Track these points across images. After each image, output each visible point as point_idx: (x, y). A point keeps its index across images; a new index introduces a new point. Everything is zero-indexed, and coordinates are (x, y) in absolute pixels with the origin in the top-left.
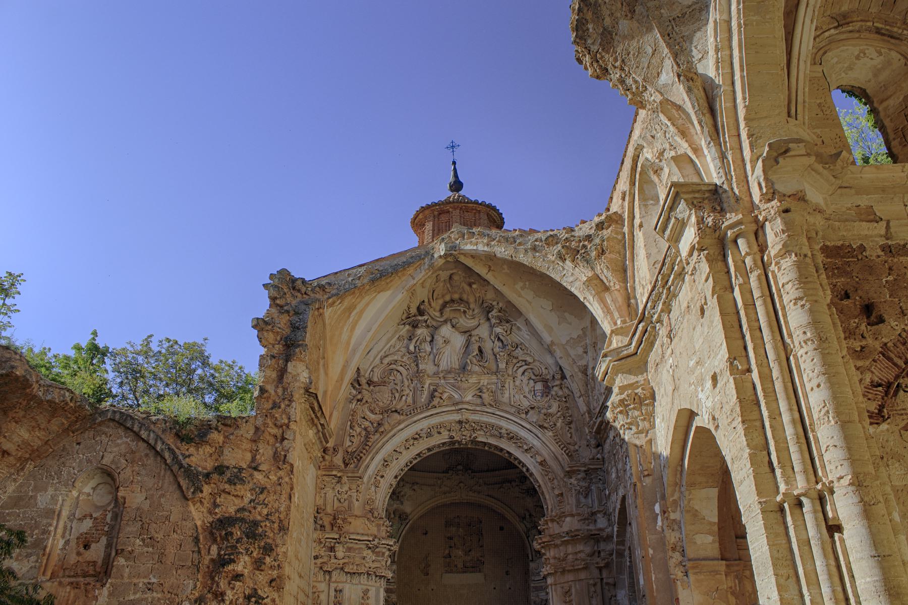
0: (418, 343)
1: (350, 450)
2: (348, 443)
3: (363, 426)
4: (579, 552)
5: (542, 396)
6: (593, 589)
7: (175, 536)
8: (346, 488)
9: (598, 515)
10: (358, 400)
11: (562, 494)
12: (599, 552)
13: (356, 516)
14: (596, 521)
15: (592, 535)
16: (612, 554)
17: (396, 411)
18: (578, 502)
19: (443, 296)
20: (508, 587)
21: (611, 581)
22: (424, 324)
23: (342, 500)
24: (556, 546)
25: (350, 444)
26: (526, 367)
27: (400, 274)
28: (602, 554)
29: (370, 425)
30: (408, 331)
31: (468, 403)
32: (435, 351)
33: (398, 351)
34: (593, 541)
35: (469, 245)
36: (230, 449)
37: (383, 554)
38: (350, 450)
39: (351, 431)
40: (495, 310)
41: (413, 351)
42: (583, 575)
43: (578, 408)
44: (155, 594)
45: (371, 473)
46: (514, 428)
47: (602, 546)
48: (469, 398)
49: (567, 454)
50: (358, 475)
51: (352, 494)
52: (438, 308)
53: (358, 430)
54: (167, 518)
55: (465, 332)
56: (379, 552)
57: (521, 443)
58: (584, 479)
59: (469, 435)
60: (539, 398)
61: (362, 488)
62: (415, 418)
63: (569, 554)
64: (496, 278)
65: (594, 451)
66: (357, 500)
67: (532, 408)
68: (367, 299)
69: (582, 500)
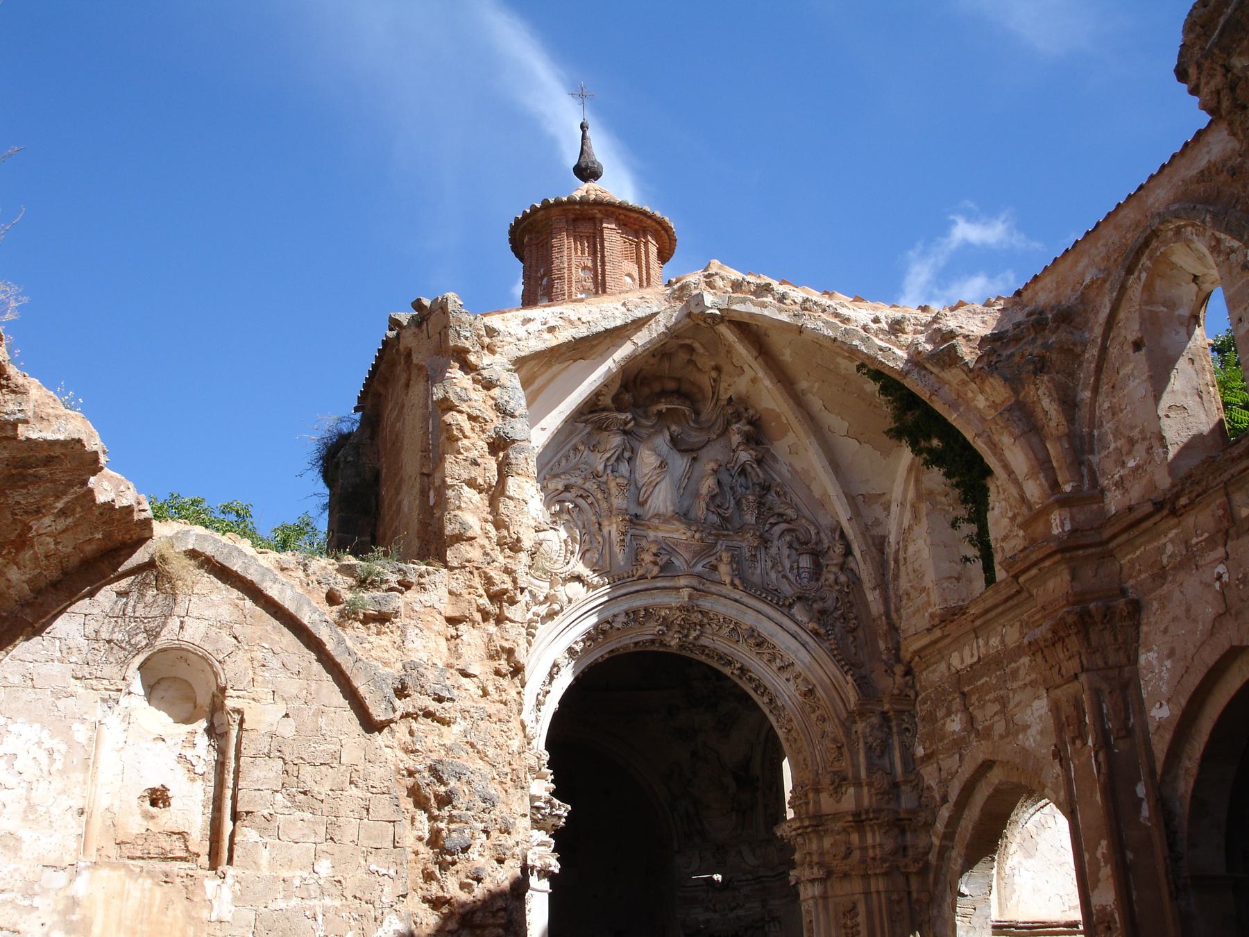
5: (810, 579)
7: (353, 791)
12: (905, 849)
14: (898, 797)
16: (927, 854)
26: (784, 526)
33: (576, 468)
36: (417, 631)
40: (744, 421)
43: (866, 604)
44: (327, 901)
46: (766, 628)
54: (336, 756)
68: (556, 368)
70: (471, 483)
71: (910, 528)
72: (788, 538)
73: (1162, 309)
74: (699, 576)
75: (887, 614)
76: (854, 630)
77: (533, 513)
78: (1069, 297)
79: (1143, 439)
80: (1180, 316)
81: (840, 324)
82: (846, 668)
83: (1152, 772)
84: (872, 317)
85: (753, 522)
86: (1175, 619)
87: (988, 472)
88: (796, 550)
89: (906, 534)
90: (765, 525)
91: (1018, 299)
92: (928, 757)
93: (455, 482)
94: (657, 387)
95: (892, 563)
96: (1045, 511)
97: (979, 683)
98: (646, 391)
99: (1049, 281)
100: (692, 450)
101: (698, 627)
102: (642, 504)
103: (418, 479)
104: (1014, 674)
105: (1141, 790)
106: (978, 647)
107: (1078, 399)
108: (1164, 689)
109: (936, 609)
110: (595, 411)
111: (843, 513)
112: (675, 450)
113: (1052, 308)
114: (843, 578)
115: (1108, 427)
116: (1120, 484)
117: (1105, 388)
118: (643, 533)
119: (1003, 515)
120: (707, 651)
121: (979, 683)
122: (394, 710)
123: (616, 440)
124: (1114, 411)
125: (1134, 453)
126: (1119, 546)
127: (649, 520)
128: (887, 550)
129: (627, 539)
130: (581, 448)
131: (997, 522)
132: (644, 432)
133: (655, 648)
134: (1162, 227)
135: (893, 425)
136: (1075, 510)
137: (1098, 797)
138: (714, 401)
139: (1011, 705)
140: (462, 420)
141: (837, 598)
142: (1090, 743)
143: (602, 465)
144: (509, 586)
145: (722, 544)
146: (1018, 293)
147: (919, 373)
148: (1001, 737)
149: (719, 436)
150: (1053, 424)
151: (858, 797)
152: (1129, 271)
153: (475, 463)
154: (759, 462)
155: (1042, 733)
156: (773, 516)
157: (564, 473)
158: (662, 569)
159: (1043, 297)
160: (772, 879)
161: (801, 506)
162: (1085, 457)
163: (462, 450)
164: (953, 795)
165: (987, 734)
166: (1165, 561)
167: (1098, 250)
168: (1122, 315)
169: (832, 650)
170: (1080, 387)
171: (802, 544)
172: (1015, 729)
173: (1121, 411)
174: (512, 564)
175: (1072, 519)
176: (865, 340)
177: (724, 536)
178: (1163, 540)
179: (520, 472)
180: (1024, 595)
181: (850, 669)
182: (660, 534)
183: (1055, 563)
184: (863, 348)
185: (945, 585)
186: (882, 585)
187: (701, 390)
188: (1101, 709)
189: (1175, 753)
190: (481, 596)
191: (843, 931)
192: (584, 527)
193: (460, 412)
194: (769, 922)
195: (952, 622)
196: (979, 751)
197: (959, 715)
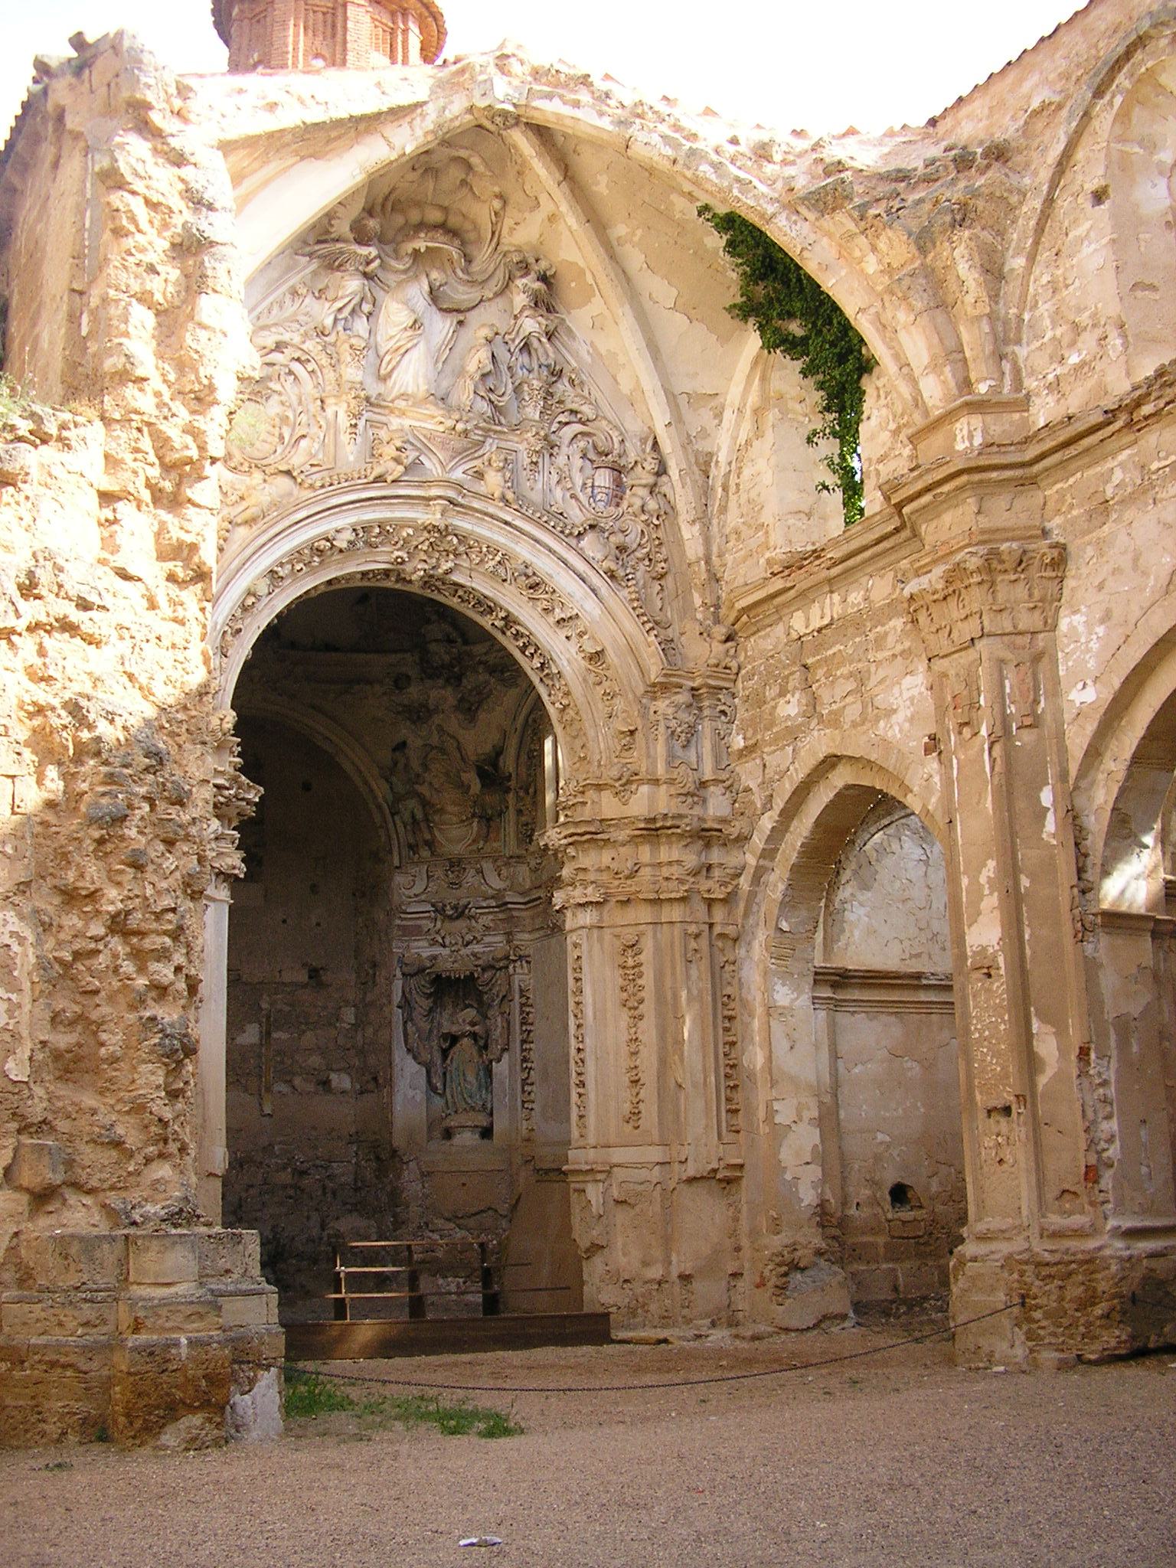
0: (346, 312)
5: (608, 504)
6: (693, 944)
9: (712, 788)
14: (704, 801)
15: (703, 830)
20: (314, 921)
21: (730, 930)
26: (578, 428)
28: (716, 873)
30: (315, 273)
34: (701, 842)
35: (556, 100)
36: (57, 506)
42: (675, 913)
43: (680, 542)
46: (544, 565)
47: (716, 856)
65: (722, 648)
68: (274, 166)
69: (679, 752)
70: (144, 298)
72: (582, 444)
73: (1137, 149)
74: (459, 486)
75: (708, 561)
76: (662, 576)
78: (1007, 129)
79: (1094, 326)
80: (1160, 163)
81: (684, 142)
82: (648, 626)
83: (1063, 776)
84: (729, 137)
85: (537, 417)
86: (1117, 571)
87: (866, 366)
89: (741, 451)
90: (551, 424)
91: (931, 130)
92: (749, 750)
93: (122, 296)
94: (415, 216)
95: (720, 490)
96: (949, 417)
97: (830, 652)
98: (399, 220)
99: (978, 107)
100: (458, 311)
101: (452, 556)
102: (384, 379)
103: (65, 298)
104: (880, 642)
105: (1046, 797)
106: (832, 604)
107: (1006, 269)
108: (1091, 664)
109: (778, 554)
111: (660, 418)
112: (434, 308)
113: (981, 143)
114: (652, 505)
115: (1045, 309)
116: (1055, 387)
117: (1044, 256)
118: (383, 419)
119: (882, 427)
120: (460, 593)
121: (830, 652)
122: (18, 616)
123: (353, 285)
124: (1054, 287)
125: (1079, 345)
126: (1047, 469)
127: (392, 401)
128: (713, 472)
129: (361, 424)
130: (303, 291)
131: (872, 437)
132: (391, 279)
133: (389, 584)
134: (1153, 32)
135: (739, 300)
136: (989, 418)
137: (989, 804)
138: (493, 244)
139: (871, 684)
140: (137, 206)
142: (984, 732)
143: (332, 318)
144: (194, 453)
145: (490, 445)
146: (933, 122)
147: (788, 219)
148: (854, 725)
149: (497, 295)
150: (970, 299)
151: (652, 799)
152: (1098, 93)
153: (152, 269)
154: (550, 336)
155: (911, 720)
157: (276, 324)
158: (407, 469)
159: (969, 130)
161: (603, 403)
162: (1009, 349)
163: (133, 251)
164: (779, 804)
165: (834, 721)
166: (1109, 493)
167: (1056, 62)
168: (1080, 155)
169: (632, 600)
170: (1011, 252)
171: (600, 454)
172: (874, 713)
173: (1067, 286)
174: (200, 422)
175: (985, 431)
176: (717, 167)
177: (496, 432)
178: (1110, 463)
179: (218, 288)
180: (906, 534)
181: (652, 629)
182: (407, 422)
183: (957, 489)
184: (713, 177)
185: (791, 522)
186: (703, 518)
187: (476, 228)
188: (1002, 686)
189: (1094, 753)
190: (152, 465)
191: (621, 971)
192: (300, 403)
193: (134, 193)
194: (514, 961)
195: (800, 568)
196: (819, 743)
197: (797, 695)
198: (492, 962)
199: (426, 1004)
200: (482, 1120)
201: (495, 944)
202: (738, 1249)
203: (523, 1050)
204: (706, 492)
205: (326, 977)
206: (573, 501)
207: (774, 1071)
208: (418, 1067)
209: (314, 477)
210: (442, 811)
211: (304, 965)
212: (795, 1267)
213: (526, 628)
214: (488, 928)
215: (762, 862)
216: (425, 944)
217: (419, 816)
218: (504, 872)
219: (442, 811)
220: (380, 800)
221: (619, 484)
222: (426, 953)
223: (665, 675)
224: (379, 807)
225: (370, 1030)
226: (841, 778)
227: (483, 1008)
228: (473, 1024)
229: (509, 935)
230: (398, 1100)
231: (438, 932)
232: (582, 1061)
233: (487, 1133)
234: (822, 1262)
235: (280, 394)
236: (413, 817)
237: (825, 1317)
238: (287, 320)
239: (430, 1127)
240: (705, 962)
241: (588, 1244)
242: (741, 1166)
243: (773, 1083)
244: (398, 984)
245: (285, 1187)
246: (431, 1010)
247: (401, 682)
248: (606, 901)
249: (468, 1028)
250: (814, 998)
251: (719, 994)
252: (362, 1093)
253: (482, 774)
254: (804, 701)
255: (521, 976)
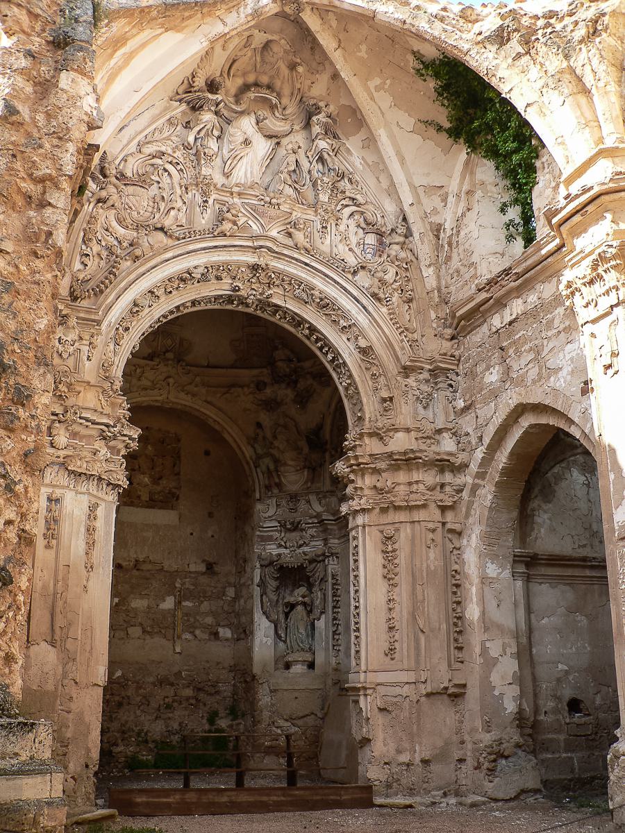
0: (202, 134)
1: (81, 277)
2: (77, 266)
3: (104, 244)
4: (417, 482)
5: (374, 255)
6: (431, 535)
8: (72, 336)
9: (445, 434)
10: (99, 201)
11: (391, 399)
13: (88, 383)
14: (438, 442)
15: (437, 460)
16: (461, 491)
17: (162, 229)
18: (416, 412)
19: (244, 74)
20: (210, 534)
21: (457, 527)
22: (213, 108)
23: (65, 355)
24: (376, 471)
25: (81, 267)
26: (354, 208)
27: (205, 10)
28: (448, 489)
29: (116, 243)
30: (183, 113)
31: (273, 240)
32: (225, 152)
33: (168, 138)
37: (119, 451)
38: (81, 277)
39: (84, 247)
40: (323, 114)
41: (192, 143)
45: (113, 320)
46: (332, 291)
47: (448, 477)
48: (274, 233)
49: (408, 341)
50: (97, 318)
51: (83, 348)
52: (233, 91)
53: (96, 248)
55: (270, 137)
56: (114, 447)
57: (337, 315)
58: (427, 381)
59: (261, 290)
60: (369, 256)
61: (99, 341)
62: (191, 247)
63: (399, 484)
64: (346, 61)
65: (449, 344)
66: (89, 359)
67: (363, 268)
68: (146, 34)
71: (463, 215)
77: (88, 109)
85: (327, 200)
88: (364, 229)
90: (337, 205)
100: (276, 137)
102: (227, 175)
104: (550, 325)
110: (190, 92)
114: (403, 255)
121: (518, 336)
127: (231, 188)
128: (442, 235)
141: (397, 273)
148: (534, 382)
156: (344, 199)
160: (333, 522)
164: (487, 441)
165: (520, 382)
181: (403, 332)
185: (490, 259)
186: (436, 264)
194: (328, 556)
196: (512, 398)
197: (497, 367)
198: (315, 558)
199: (274, 584)
200: (309, 657)
201: (316, 546)
202: (463, 742)
203: (334, 613)
204: (438, 247)
205: (216, 569)
206: (350, 253)
207: (487, 620)
208: (269, 623)
209: (178, 233)
210: (285, 464)
211: (204, 561)
212: (502, 756)
213: (322, 334)
214: (313, 536)
215: (477, 481)
216: (275, 547)
217: (272, 467)
218: (323, 501)
219: (285, 464)
220: (248, 459)
221: (381, 243)
222: (275, 552)
223: (411, 361)
224: (248, 463)
225: (242, 601)
226: (527, 421)
227: (310, 587)
228: (304, 597)
229: (325, 540)
230: (257, 642)
231: (282, 540)
232: (358, 614)
233: (311, 665)
234: (520, 752)
235: (159, 183)
236: (268, 469)
237: (523, 791)
238: (164, 139)
239: (276, 662)
240: (439, 548)
241: (360, 738)
242: (464, 686)
243: (486, 629)
244: (257, 573)
245: (188, 699)
246: (278, 588)
247: (260, 386)
248: (373, 508)
249: (300, 599)
250: (513, 572)
251: (449, 571)
252: (238, 640)
253: (309, 441)
254: (501, 372)
255: (332, 566)
